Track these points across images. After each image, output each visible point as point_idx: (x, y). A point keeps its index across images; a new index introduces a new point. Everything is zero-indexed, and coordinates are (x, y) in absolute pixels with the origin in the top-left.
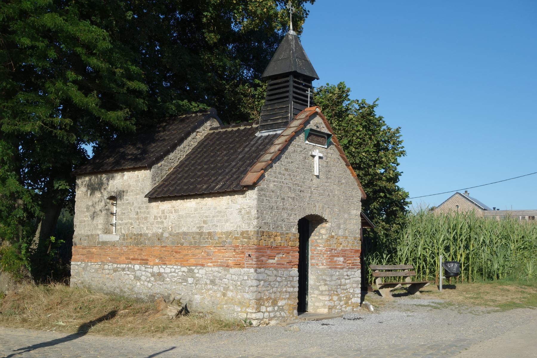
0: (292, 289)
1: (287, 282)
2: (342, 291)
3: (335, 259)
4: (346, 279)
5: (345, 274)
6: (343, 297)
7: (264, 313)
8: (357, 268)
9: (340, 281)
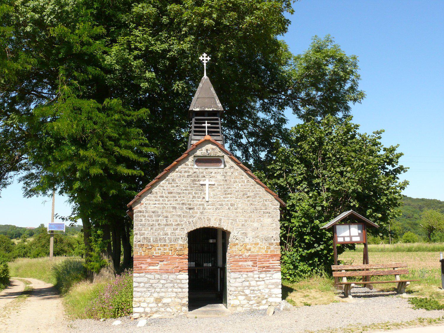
0: (180, 290)
2: (252, 292)
3: (240, 263)
4: (257, 281)
5: (257, 276)
8: (275, 270)
9: (248, 282)
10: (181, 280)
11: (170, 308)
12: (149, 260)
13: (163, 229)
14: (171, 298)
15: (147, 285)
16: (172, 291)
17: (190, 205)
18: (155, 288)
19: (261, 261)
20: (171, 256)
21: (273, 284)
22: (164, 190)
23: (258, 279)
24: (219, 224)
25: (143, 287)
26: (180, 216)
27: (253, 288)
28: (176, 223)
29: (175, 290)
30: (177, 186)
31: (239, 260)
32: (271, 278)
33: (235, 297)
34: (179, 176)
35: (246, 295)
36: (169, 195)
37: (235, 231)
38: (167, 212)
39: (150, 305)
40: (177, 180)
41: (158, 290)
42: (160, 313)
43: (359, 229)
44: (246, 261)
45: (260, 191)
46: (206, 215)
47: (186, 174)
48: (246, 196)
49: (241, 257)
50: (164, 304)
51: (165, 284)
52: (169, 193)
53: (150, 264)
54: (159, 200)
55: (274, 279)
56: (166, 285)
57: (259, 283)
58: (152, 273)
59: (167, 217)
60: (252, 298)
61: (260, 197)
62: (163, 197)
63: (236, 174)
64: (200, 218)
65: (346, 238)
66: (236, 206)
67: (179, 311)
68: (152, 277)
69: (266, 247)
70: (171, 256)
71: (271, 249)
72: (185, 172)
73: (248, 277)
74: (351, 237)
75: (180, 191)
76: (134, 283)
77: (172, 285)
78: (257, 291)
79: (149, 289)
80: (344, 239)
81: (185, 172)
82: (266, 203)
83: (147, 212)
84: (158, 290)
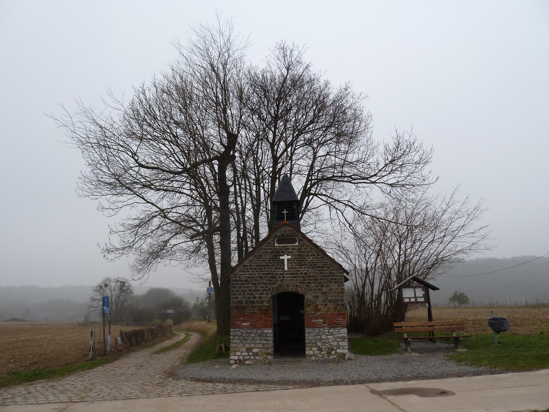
0: (266, 342)
1: (261, 337)
2: (323, 344)
3: (313, 321)
4: (327, 335)
5: (327, 331)
6: (325, 348)
7: (239, 356)
8: (342, 326)
10: (266, 334)
11: (258, 356)
12: (242, 318)
13: (253, 294)
14: (259, 348)
15: (241, 338)
16: (260, 343)
17: (273, 274)
18: (247, 340)
19: (330, 319)
20: (258, 315)
21: (340, 338)
22: (253, 263)
23: (327, 334)
24: (295, 289)
25: (238, 339)
26: (265, 283)
27: (324, 341)
28: (262, 289)
29: (262, 342)
30: (263, 260)
31: (312, 318)
32: (339, 333)
33: (309, 348)
34: (264, 252)
35: (318, 347)
36: (257, 267)
37: (308, 294)
38: (255, 280)
39: (243, 354)
40: (263, 256)
41: (249, 342)
42: (251, 360)
43: (423, 291)
44: (317, 319)
45: (327, 262)
46: (285, 282)
47: (270, 251)
48: (316, 266)
49: (313, 316)
50: (253, 353)
51: (254, 337)
52: (257, 266)
53: (243, 321)
54: (249, 272)
55: (341, 333)
56: (255, 338)
57: (328, 337)
58: (245, 329)
59: (255, 284)
60: (323, 349)
61: (328, 267)
62: (252, 269)
63: (309, 249)
64: (280, 285)
65: (411, 299)
66: (308, 275)
67: (265, 359)
68: (244, 331)
69: (333, 307)
70: (258, 315)
71: (338, 309)
72: (269, 249)
73: (320, 332)
74: (416, 297)
75: (265, 264)
76: (231, 336)
77: (259, 338)
78: (327, 343)
79: (242, 341)
80: (410, 300)
81: (269, 249)
82: (333, 272)
83: (240, 281)
84: (249, 342)
